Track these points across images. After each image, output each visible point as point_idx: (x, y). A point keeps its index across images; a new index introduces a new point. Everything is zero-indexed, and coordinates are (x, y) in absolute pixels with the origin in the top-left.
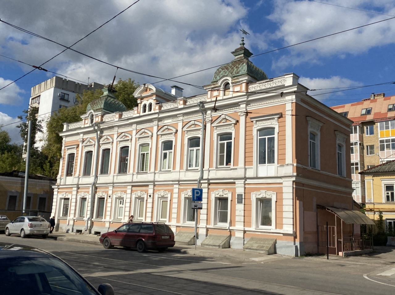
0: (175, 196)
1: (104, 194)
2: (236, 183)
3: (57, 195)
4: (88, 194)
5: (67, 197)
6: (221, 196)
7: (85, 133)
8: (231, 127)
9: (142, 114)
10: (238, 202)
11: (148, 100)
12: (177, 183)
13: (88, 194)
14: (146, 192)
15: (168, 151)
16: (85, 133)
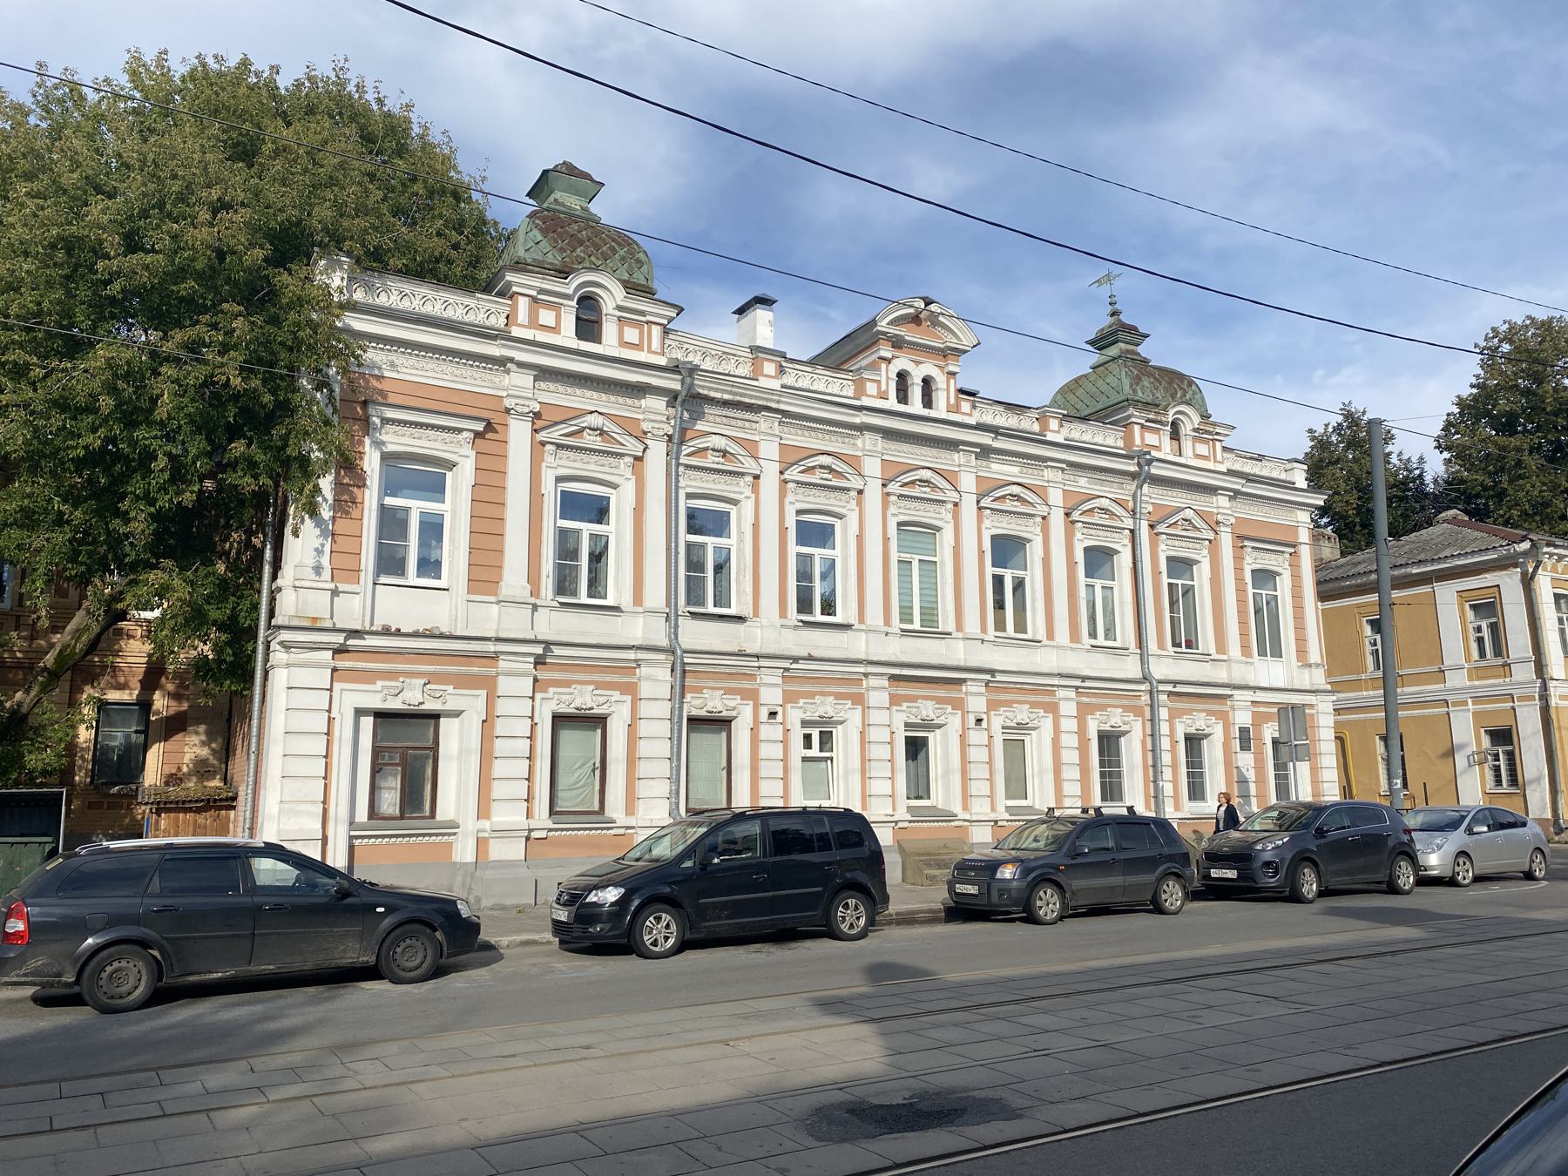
0: (1069, 725)
1: (732, 704)
2: (1236, 698)
3: (331, 690)
4: (628, 698)
5: (430, 706)
6: (412, 707)
7: (544, 374)
8: (1198, 546)
9: (892, 403)
10: (1242, 748)
11: (918, 363)
12: (1078, 683)
13: (628, 698)
14: (958, 704)
15: (1011, 571)
16: (544, 374)
